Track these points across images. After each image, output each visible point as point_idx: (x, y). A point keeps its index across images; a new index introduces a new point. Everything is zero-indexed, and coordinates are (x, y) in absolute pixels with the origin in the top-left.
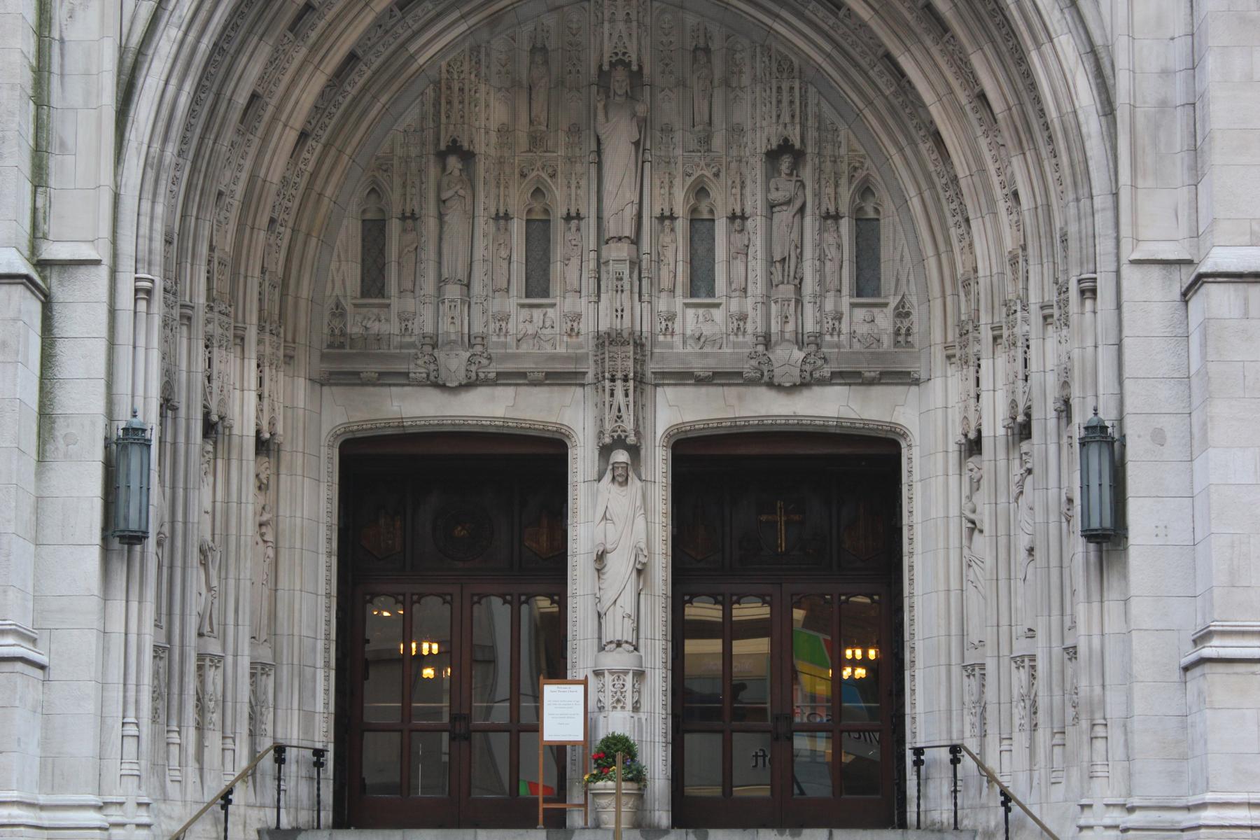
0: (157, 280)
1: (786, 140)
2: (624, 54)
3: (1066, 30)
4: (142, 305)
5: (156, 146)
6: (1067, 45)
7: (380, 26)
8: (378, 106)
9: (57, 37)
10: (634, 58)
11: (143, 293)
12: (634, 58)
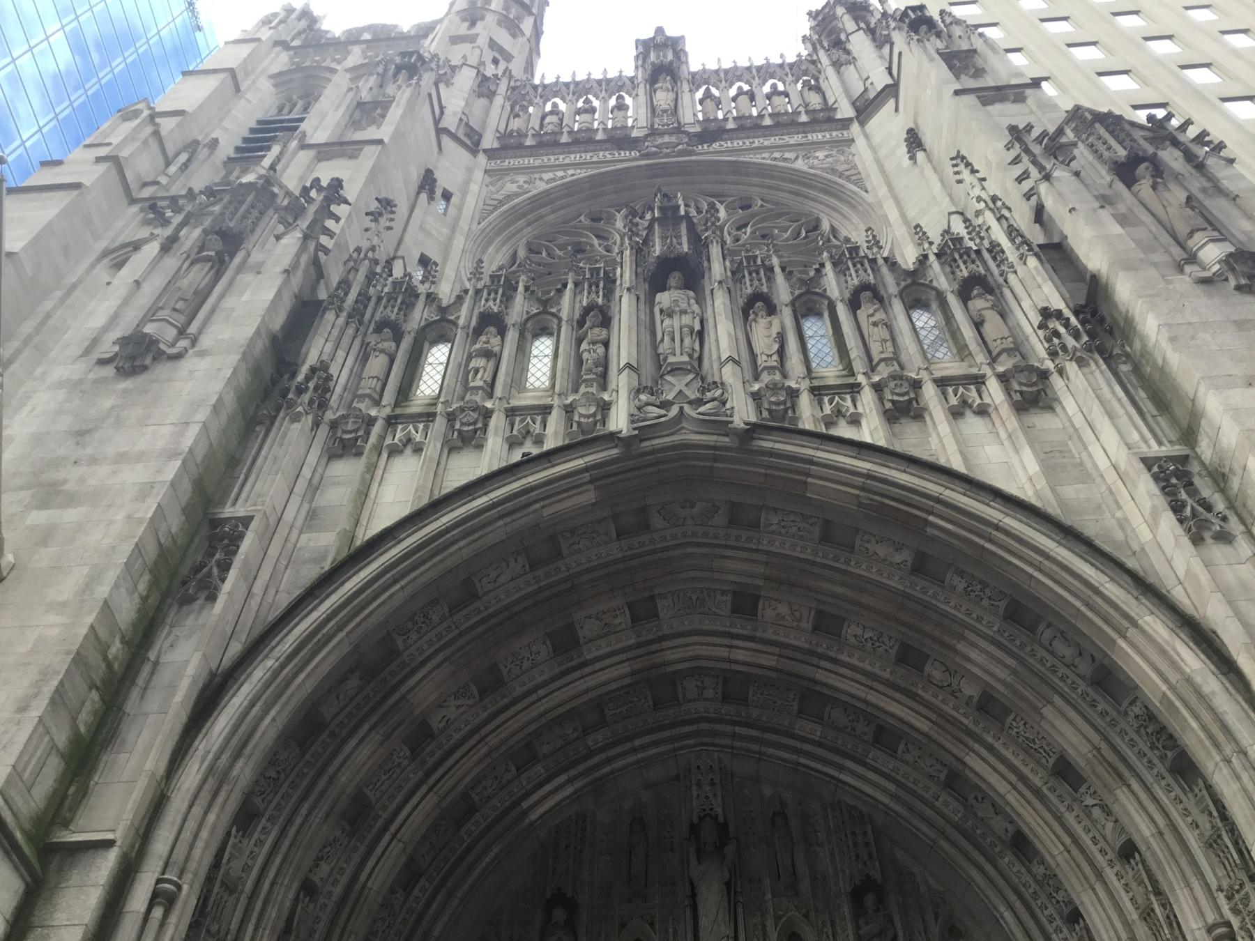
0: (185, 887)
1: (868, 876)
2: (711, 809)
3: (1148, 612)
4: (158, 913)
5: (225, 757)
6: (1156, 625)
7: (496, 778)
8: (491, 855)
9: (152, 658)
10: (719, 810)
11: (163, 898)
12: (719, 810)
